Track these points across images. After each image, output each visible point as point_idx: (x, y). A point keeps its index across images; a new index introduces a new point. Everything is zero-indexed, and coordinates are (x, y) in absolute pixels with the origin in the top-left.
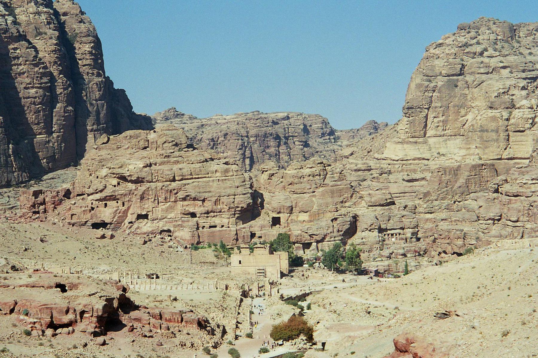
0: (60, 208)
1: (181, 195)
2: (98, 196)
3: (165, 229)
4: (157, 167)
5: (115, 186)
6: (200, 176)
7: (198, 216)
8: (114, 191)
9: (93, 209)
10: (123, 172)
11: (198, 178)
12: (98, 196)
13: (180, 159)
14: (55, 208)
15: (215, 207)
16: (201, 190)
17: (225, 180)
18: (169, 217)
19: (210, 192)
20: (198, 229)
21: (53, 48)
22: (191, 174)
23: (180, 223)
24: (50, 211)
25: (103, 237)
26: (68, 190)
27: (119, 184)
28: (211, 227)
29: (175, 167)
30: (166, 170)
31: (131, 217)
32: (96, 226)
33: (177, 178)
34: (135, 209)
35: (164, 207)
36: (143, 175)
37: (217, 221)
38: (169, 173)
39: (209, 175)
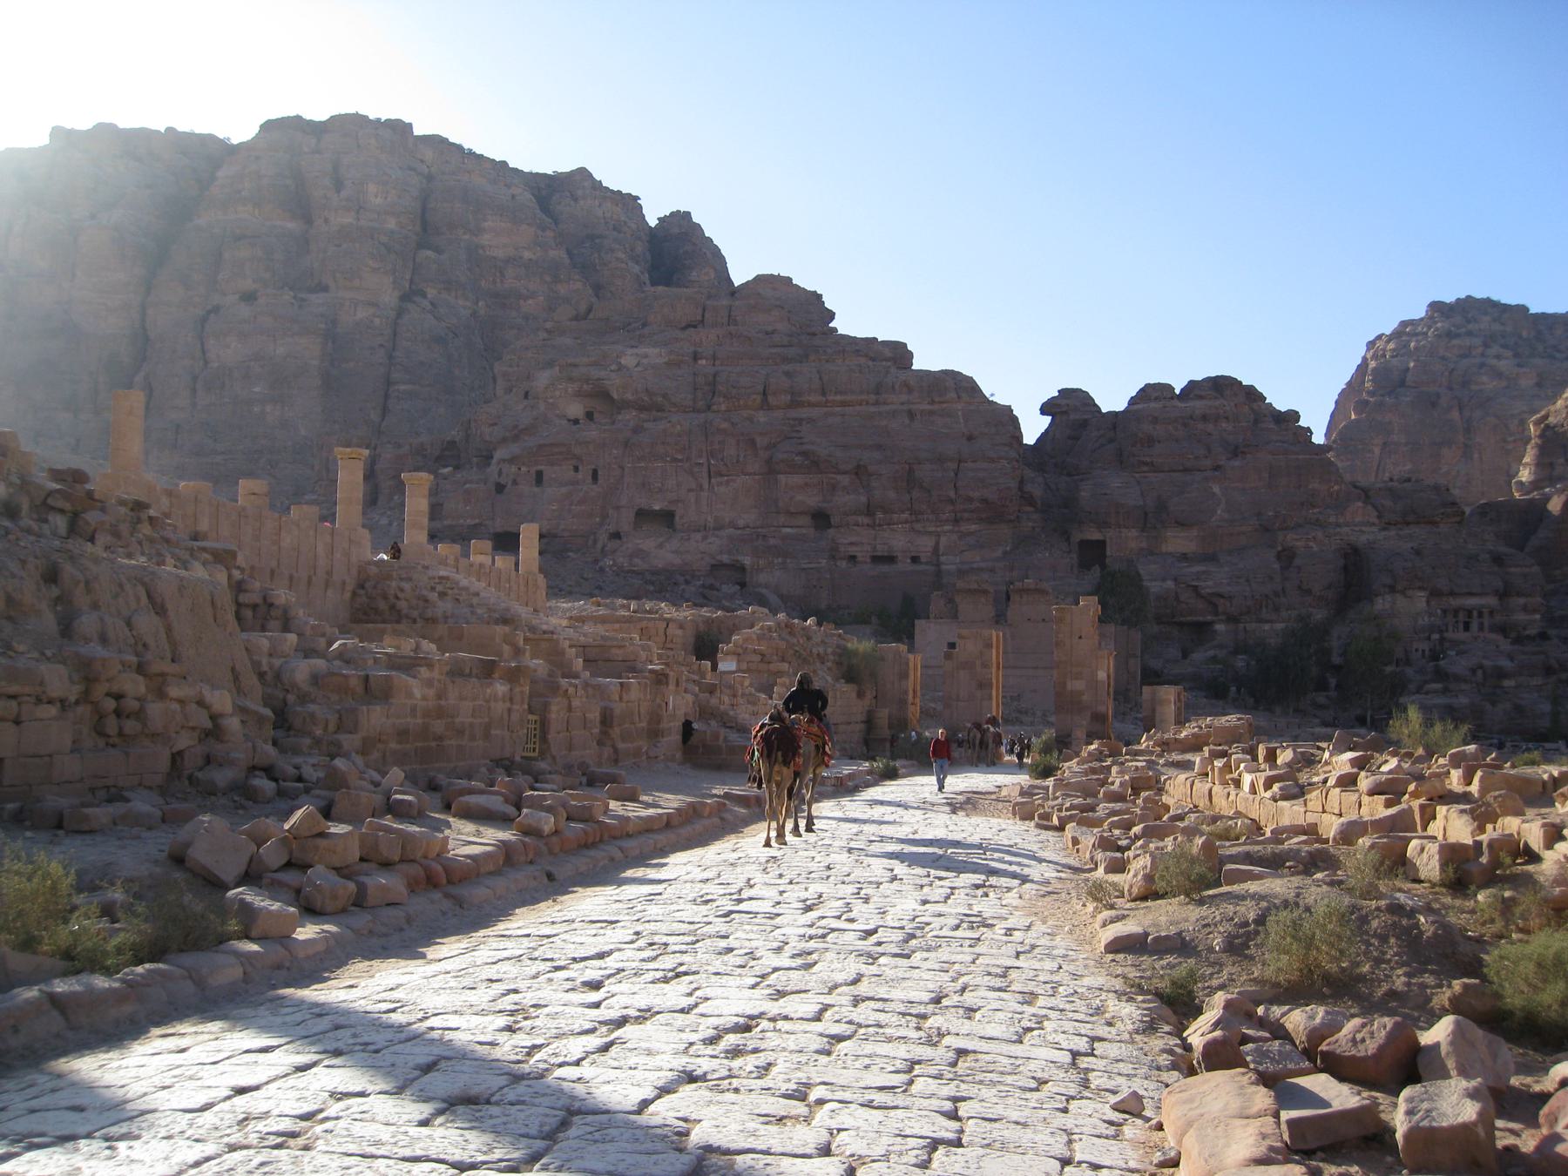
2: (515, 449)
5: (576, 422)
6: (848, 398)
7: (835, 520)
10: (603, 374)
11: (844, 404)
15: (892, 494)
17: (931, 413)
18: (741, 523)
19: (879, 447)
23: (772, 541)
26: (452, 443)
27: (589, 416)
28: (877, 559)
35: (723, 489)
37: (897, 540)
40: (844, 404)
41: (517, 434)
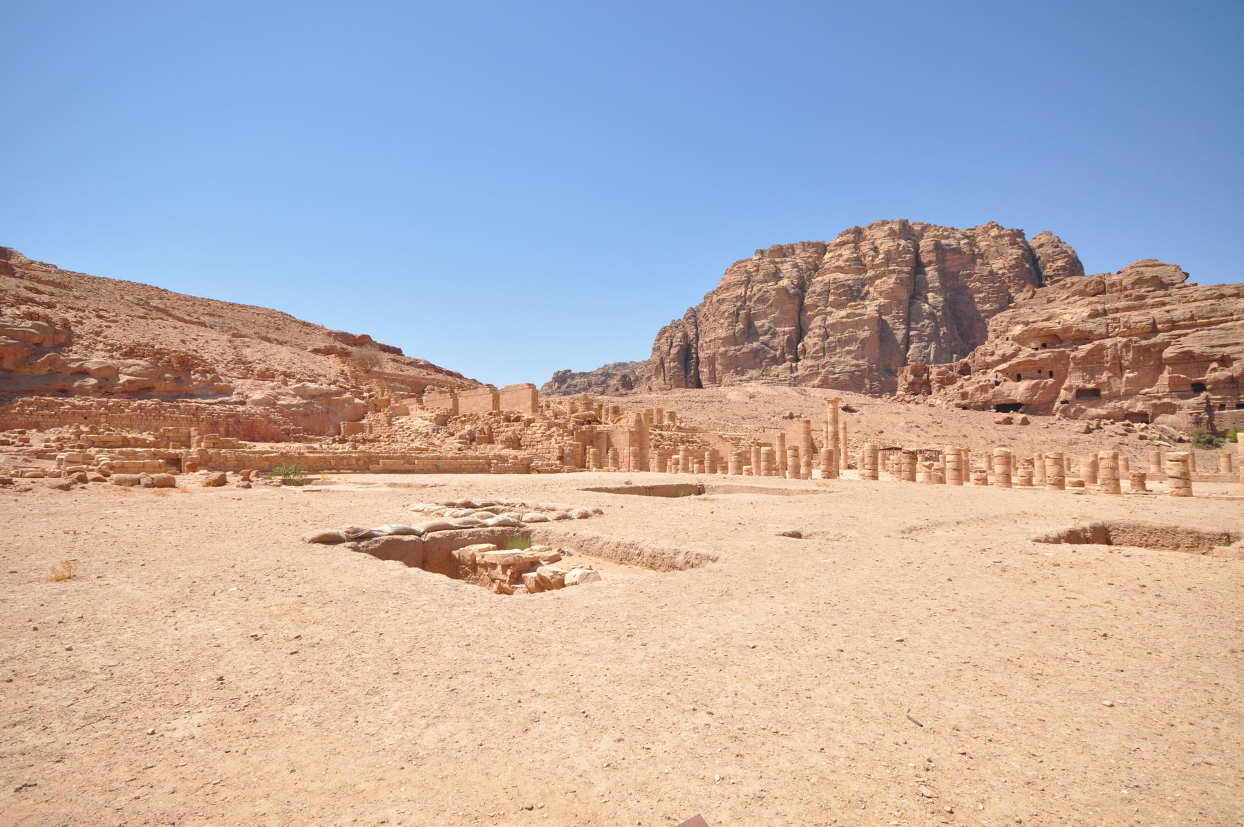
0: (949, 388)
1: (1168, 353)
2: (1004, 366)
3: (1136, 410)
4: (1118, 315)
8: (1034, 355)
9: (997, 383)
12: (1004, 366)
13: (1167, 299)
14: (940, 388)
16: (1215, 342)
19: (1237, 344)
20: (1209, 409)
21: (1013, 262)
22: (1192, 318)
24: (934, 391)
25: (1008, 421)
26: (966, 364)
29: (1156, 313)
30: (1137, 318)
31: (1063, 394)
32: (1002, 408)
33: (1159, 326)
34: (1075, 380)
36: (1090, 325)
38: (1139, 319)
39: (1235, 317)
40: (1210, 324)
41: (1004, 359)
